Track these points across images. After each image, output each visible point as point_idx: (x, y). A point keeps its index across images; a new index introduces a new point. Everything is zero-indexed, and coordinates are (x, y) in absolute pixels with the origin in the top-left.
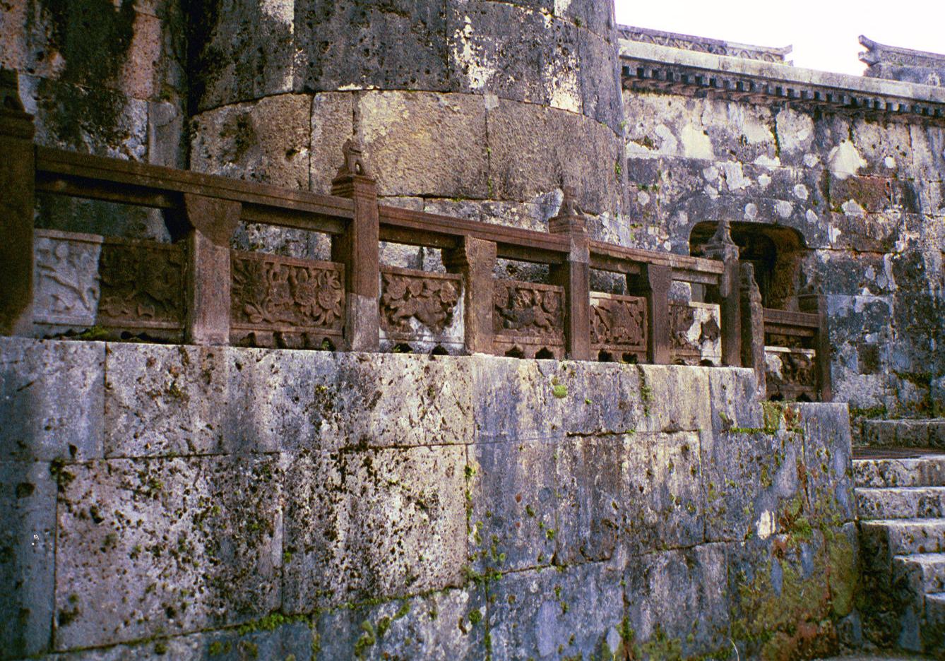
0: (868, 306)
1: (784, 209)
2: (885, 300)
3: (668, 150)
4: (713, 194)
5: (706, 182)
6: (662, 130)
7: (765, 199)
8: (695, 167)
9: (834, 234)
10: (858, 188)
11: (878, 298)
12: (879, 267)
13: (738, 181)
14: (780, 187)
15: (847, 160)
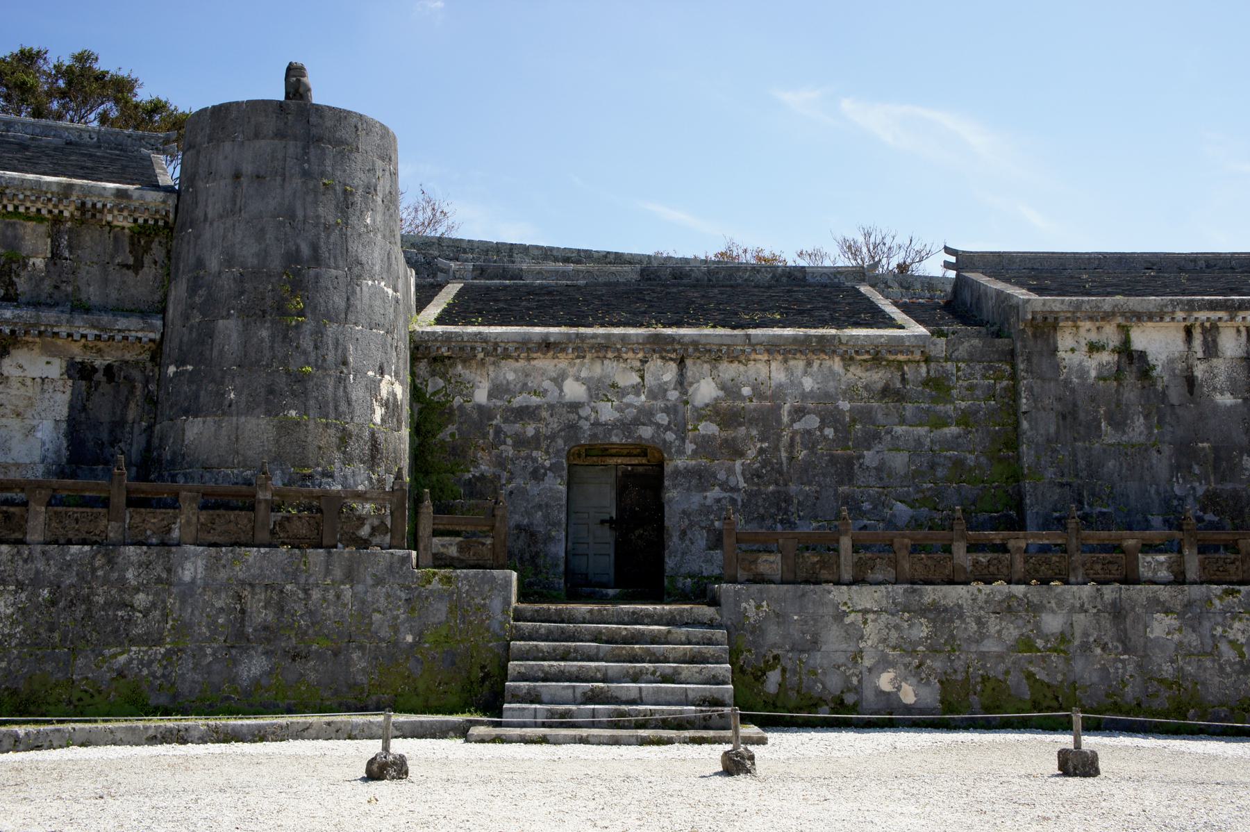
0: (718, 501)
1: (646, 432)
2: (735, 496)
3: (553, 397)
4: (585, 425)
5: (580, 418)
6: (547, 384)
7: (626, 426)
8: (575, 406)
9: (690, 447)
10: (715, 412)
11: (727, 495)
12: (731, 471)
13: (607, 413)
14: (645, 416)
15: (706, 391)
